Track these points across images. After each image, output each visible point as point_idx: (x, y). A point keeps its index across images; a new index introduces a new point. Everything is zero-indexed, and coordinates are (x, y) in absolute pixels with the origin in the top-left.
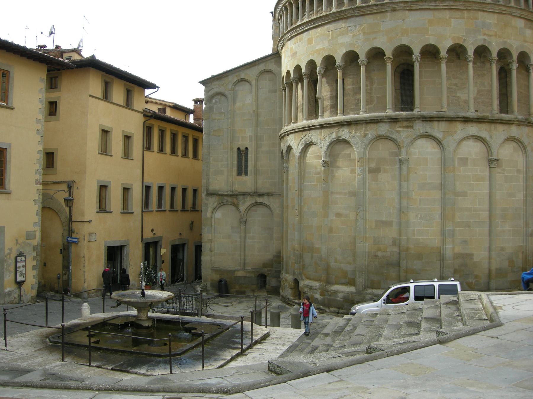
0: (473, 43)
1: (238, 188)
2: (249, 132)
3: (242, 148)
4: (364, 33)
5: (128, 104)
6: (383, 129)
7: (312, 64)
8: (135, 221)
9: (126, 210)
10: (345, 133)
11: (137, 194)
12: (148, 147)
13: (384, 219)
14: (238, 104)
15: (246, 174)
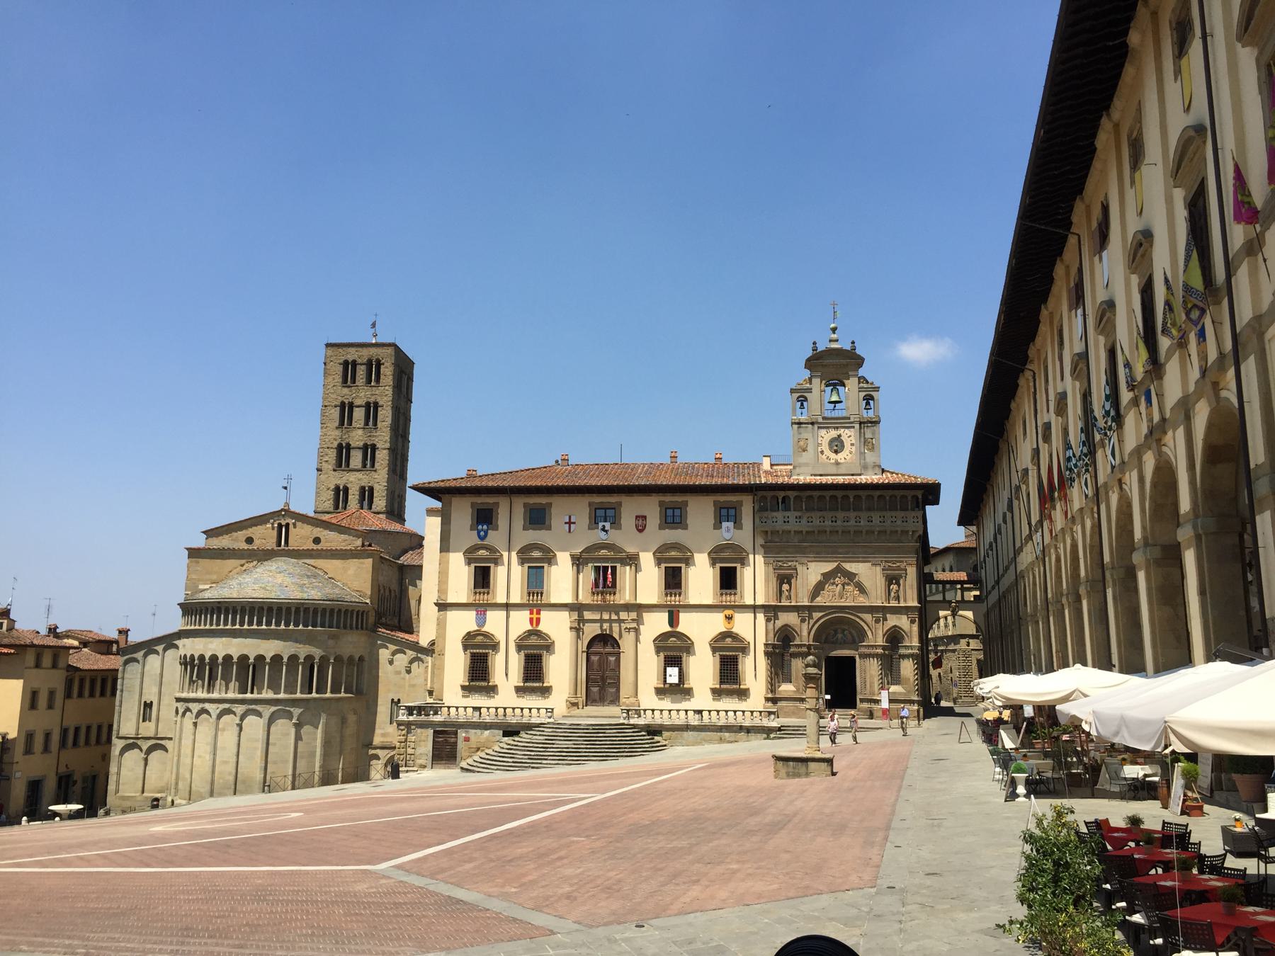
0: (288, 654)
1: (143, 733)
2: (155, 690)
3: (148, 702)
4: (223, 645)
5: (54, 666)
6: (227, 706)
7: (192, 656)
8: (50, 760)
9: (46, 749)
10: (207, 706)
11: (56, 738)
12: (68, 695)
13: (225, 760)
14: (147, 668)
15: (150, 721)
